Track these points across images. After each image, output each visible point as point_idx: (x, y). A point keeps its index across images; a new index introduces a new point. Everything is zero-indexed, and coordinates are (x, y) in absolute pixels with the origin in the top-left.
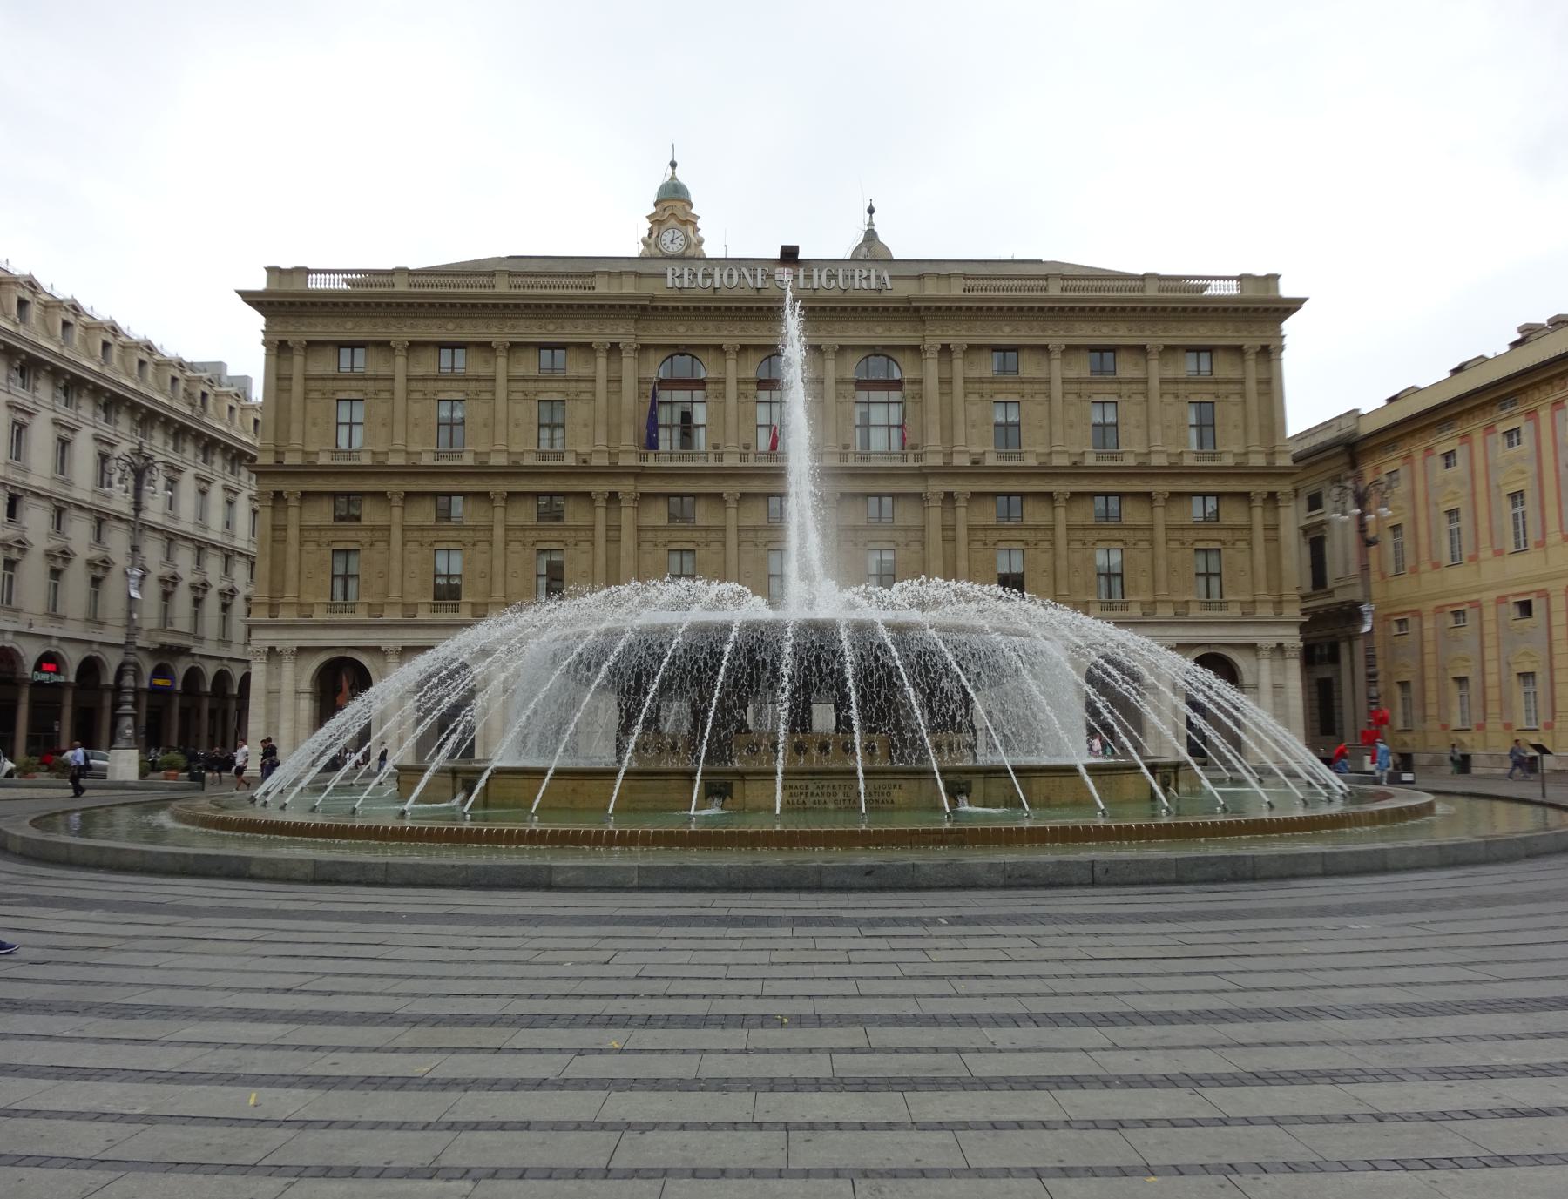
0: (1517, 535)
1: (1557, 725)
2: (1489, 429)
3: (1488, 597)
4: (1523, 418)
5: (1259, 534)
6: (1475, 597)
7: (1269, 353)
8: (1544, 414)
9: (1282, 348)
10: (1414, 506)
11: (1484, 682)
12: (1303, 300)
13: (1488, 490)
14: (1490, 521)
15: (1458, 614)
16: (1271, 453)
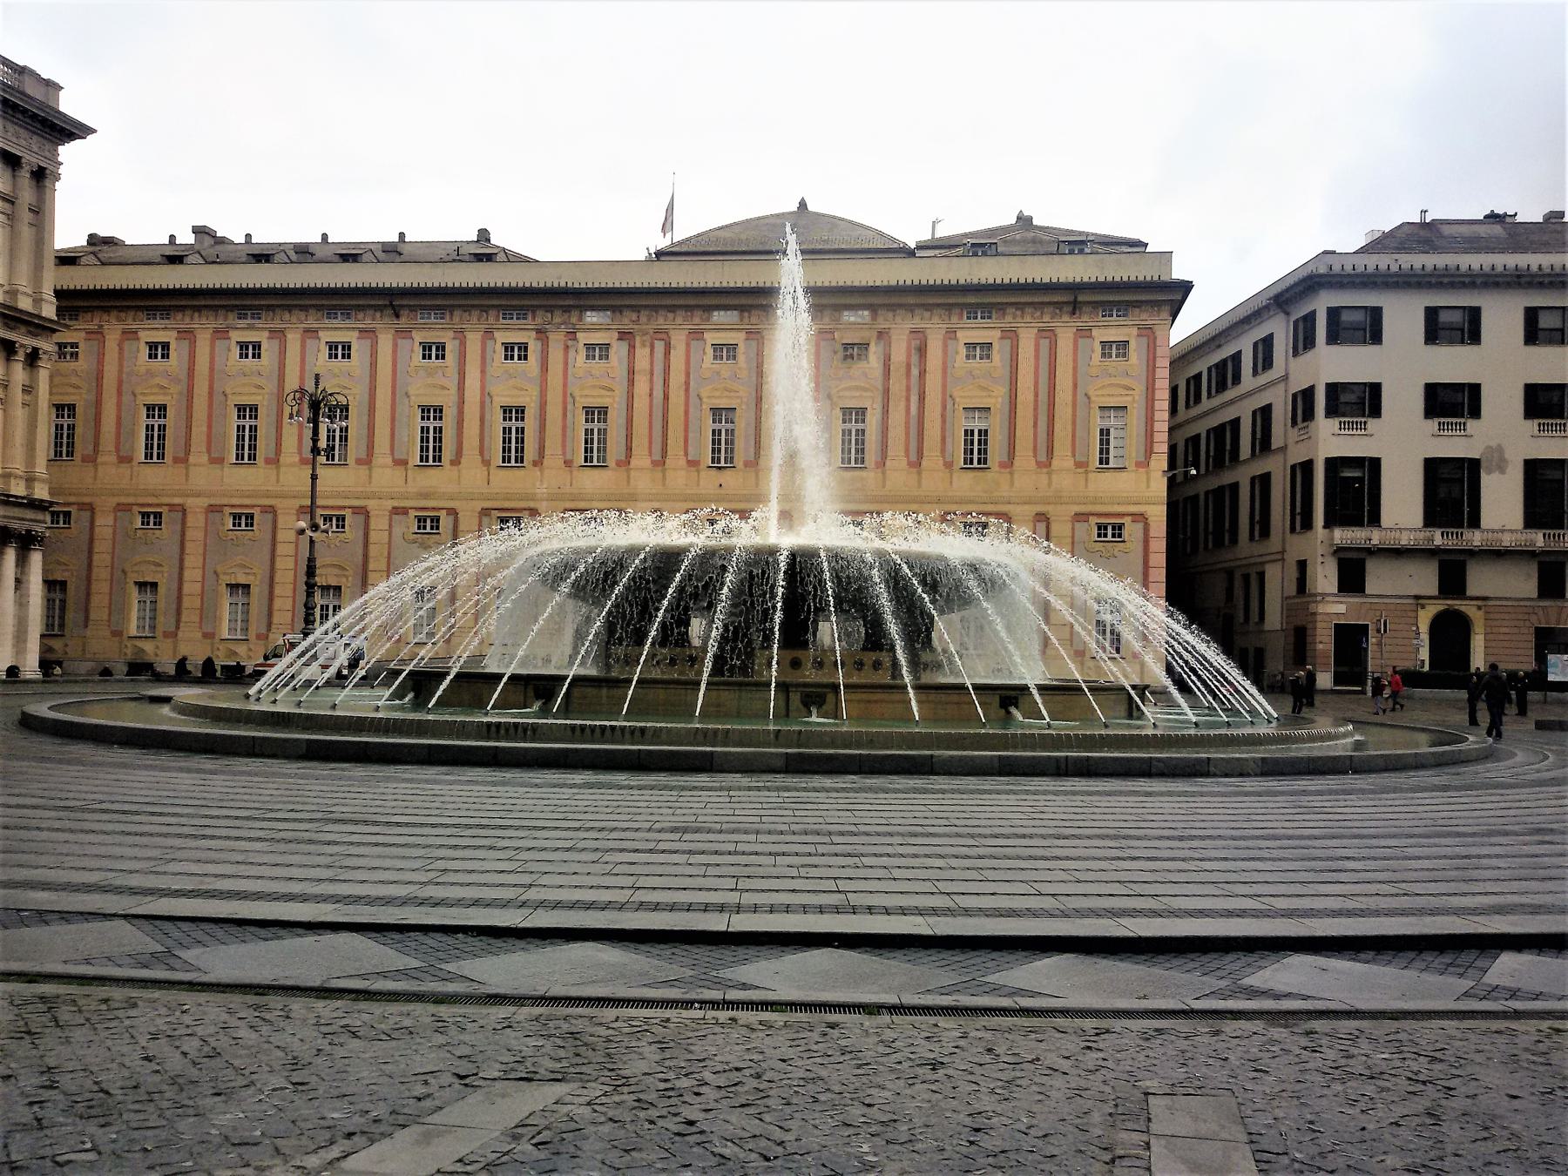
0: (240, 447)
1: (180, 634)
2: (221, 334)
3: (196, 504)
4: (266, 334)
5: (18, 396)
6: (177, 501)
7: (43, 176)
8: (293, 339)
9: (57, 177)
10: (99, 393)
11: (180, 589)
12: (94, 131)
13: (211, 394)
14: (210, 427)
15: (153, 518)
16: (38, 301)
